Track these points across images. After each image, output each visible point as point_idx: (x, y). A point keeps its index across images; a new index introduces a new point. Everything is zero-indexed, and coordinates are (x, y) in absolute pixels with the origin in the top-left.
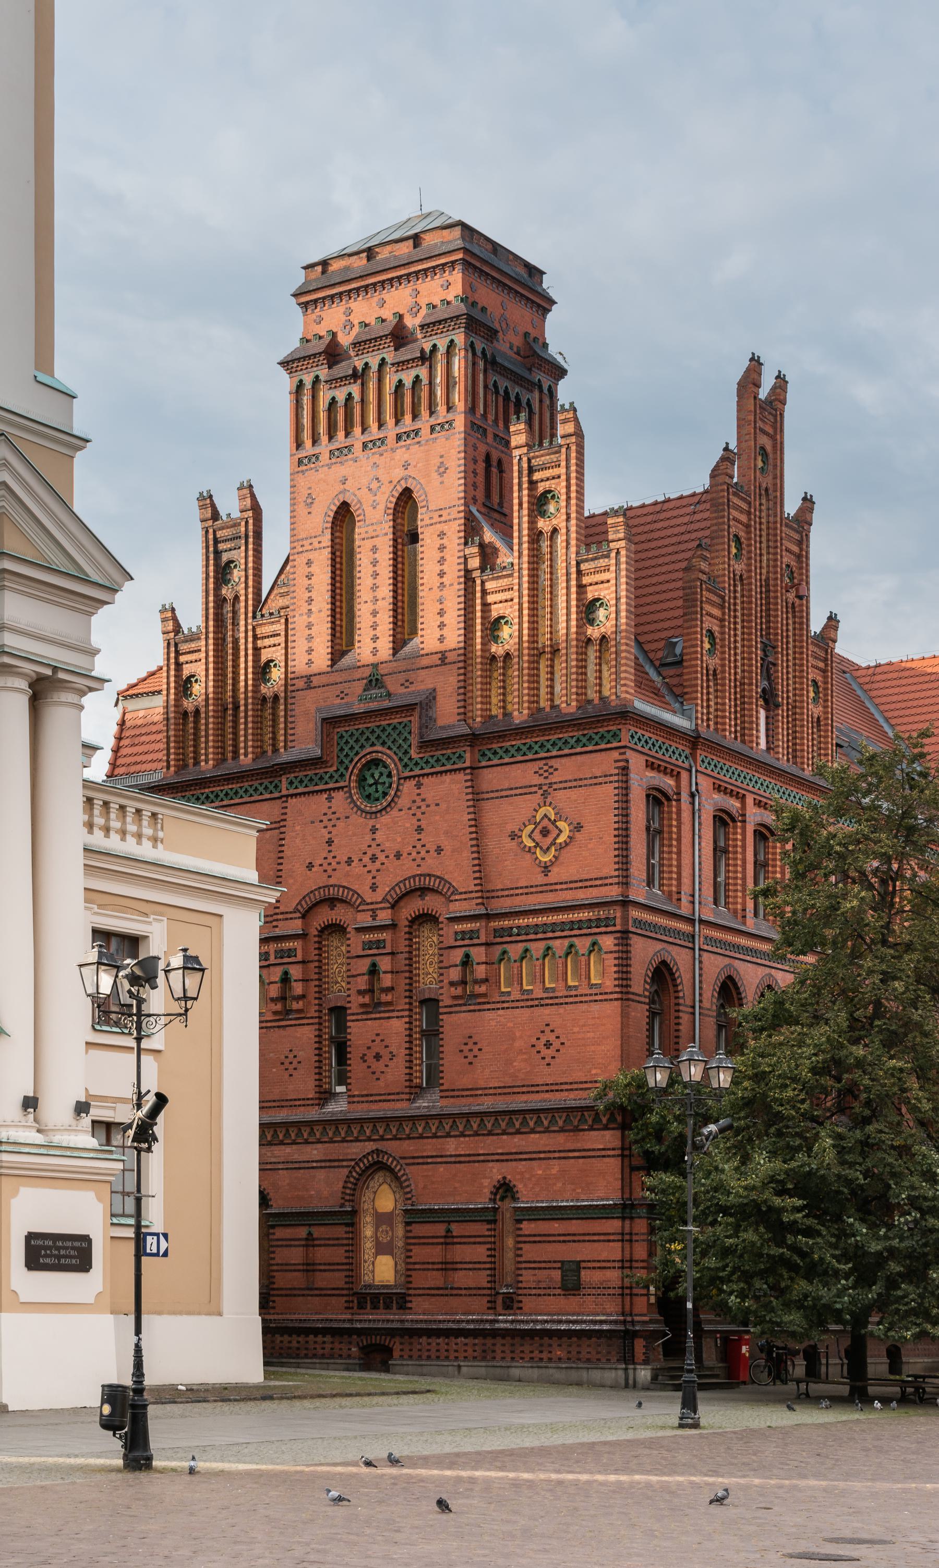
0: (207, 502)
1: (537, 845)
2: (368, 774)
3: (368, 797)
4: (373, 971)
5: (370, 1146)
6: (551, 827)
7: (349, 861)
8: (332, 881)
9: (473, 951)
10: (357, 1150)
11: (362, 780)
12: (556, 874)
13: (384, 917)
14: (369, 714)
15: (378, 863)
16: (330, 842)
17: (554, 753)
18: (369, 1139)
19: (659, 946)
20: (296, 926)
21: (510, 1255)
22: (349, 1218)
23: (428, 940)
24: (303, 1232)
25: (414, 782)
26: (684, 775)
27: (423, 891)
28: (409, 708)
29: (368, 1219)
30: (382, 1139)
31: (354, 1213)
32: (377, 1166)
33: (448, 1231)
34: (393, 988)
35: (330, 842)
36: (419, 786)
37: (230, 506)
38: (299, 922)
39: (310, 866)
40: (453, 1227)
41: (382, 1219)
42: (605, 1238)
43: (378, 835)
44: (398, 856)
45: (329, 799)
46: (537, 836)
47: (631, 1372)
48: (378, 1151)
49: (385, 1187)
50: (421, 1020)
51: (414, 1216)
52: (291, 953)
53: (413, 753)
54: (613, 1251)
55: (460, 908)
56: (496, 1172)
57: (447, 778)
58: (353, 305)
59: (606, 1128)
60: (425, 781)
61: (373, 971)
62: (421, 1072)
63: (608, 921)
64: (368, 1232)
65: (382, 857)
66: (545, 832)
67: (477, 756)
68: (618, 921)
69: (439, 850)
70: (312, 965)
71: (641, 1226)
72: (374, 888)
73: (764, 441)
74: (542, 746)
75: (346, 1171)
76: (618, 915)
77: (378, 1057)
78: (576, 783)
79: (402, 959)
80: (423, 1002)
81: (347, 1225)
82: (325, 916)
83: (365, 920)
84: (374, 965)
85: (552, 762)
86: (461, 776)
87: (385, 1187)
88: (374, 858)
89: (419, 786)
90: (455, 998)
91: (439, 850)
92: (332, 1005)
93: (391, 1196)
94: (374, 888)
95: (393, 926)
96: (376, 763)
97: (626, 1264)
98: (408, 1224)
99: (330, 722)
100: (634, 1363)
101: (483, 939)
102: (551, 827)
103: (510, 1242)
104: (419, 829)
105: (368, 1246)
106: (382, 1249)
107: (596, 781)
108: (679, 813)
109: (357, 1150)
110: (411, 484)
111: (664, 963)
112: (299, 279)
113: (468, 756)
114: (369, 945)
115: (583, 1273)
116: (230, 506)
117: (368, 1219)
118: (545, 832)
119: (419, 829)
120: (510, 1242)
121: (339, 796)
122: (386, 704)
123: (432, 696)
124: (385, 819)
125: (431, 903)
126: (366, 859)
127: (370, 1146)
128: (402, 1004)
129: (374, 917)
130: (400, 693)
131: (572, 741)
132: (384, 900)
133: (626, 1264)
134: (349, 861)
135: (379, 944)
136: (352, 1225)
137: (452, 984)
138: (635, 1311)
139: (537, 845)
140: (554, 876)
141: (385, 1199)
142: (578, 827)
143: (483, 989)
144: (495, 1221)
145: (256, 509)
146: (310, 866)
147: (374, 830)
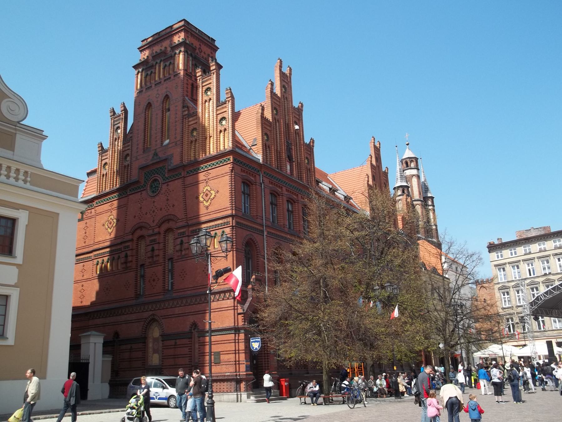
0: (113, 112)
1: (204, 200)
2: (153, 184)
3: (153, 192)
4: (153, 250)
5: (151, 313)
6: (208, 193)
7: (146, 214)
8: (141, 221)
9: (183, 239)
10: (146, 315)
11: (151, 186)
12: (211, 209)
13: (156, 230)
14: (153, 164)
15: (155, 213)
16: (141, 208)
17: (210, 168)
18: (151, 311)
19: (248, 233)
20: (130, 237)
21: (197, 351)
22: (143, 340)
23: (171, 237)
24: (129, 346)
25: (166, 184)
26: (257, 176)
27: (168, 220)
28: (166, 160)
29: (151, 340)
30: (155, 310)
31: (145, 338)
32: (153, 320)
33: (176, 343)
34: (159, 255)
35: (141, 208)
36: (168, 185)
37: (118, 111)
38: (131, 236)
39: (135, 217)
40: (177, 341)
41: (155, 340)
42: (228, 342)
43: (155, 204)
44: (161, 209)
45: (141, 194)
46: (204, 197)
47: (239, 396)
48: (153, 315)
49: (156, 328)
50: (168, 266)
51: (165, 337)
52: (128, 247)
53: (166, 176)
54: (231, 347)
55: (180, 224)
56: (191, 319)
57: (176, 181)
58: (154, 48)
59: (228, 299)
60: (169, 183)
61: (153, 250)
62: (168, 284)
63: (228, 223)
64: (151, 345)
65: (156, 211)
66: (207, 195)
67: (186, 173)
68: (231, 223)
69: (173, 206)
70: (134, 251)
71: (242, 336)
72: (153, 221)
73: (284, 83)
74: (206, 167)
75: (142, 323)
76: (231, 220)
77: (154, 280)
78: (217, 177)
79: (162, 245)
80: (169, 260)
81: (143, 343)
82: (139, 233)
83: (151, 232)
84: (153, 248)
85: (208, 171)
86: (180, 180)
87: (156, 328)
88: (154, 211)
89: (168, 185)
90: (178, 256)
91: (173, 206)
92: (141, 263)
93: (158, 331)
94: (153, 221)
95: (159, 233)
96: (156, 180)
97: (236, 352)
98: (163, 341)
99: (142, 168)
100: (240, 392)
101: (187, 234)
102: (208, 193)
103: (197, 346)
104: (168, 200)
105: (150, 350)
106: (155, 351)
107: (223, 175)
108: (256, 189)
109: (146, 315)
110: (168, 93)
111: (251, 239)
112: (140, 44)
113: (183, 173)
114: (152, 241)
115: (221, 356)
116: (118, 111)
117: (151, 340)
118: (207, 195)
119: (168, 200)
120: (197, 346)
121: (144, 192)
122: (158, 160)
123: (172, 155)
124: (157, 198)
125: (171, 225)
126: (151, 212)
127: (151, 313)
128: (161, 260)
129: (153, 231)
130: (162, 156)
131: (215, 164)
132: (157, 225)
133: (236, 352)
134: (146, 214)
135: (154, 240)
136: (145, 343)
137: (177, 251)
138: (241, 370)
139: (204, 200)
140: (209, 210)
141: (156, 332)
142: (218, 192)
143: (187, 252)
144: (191, 338)
145: (125, 111)
146: (135, 217)
147: (154, 202)
